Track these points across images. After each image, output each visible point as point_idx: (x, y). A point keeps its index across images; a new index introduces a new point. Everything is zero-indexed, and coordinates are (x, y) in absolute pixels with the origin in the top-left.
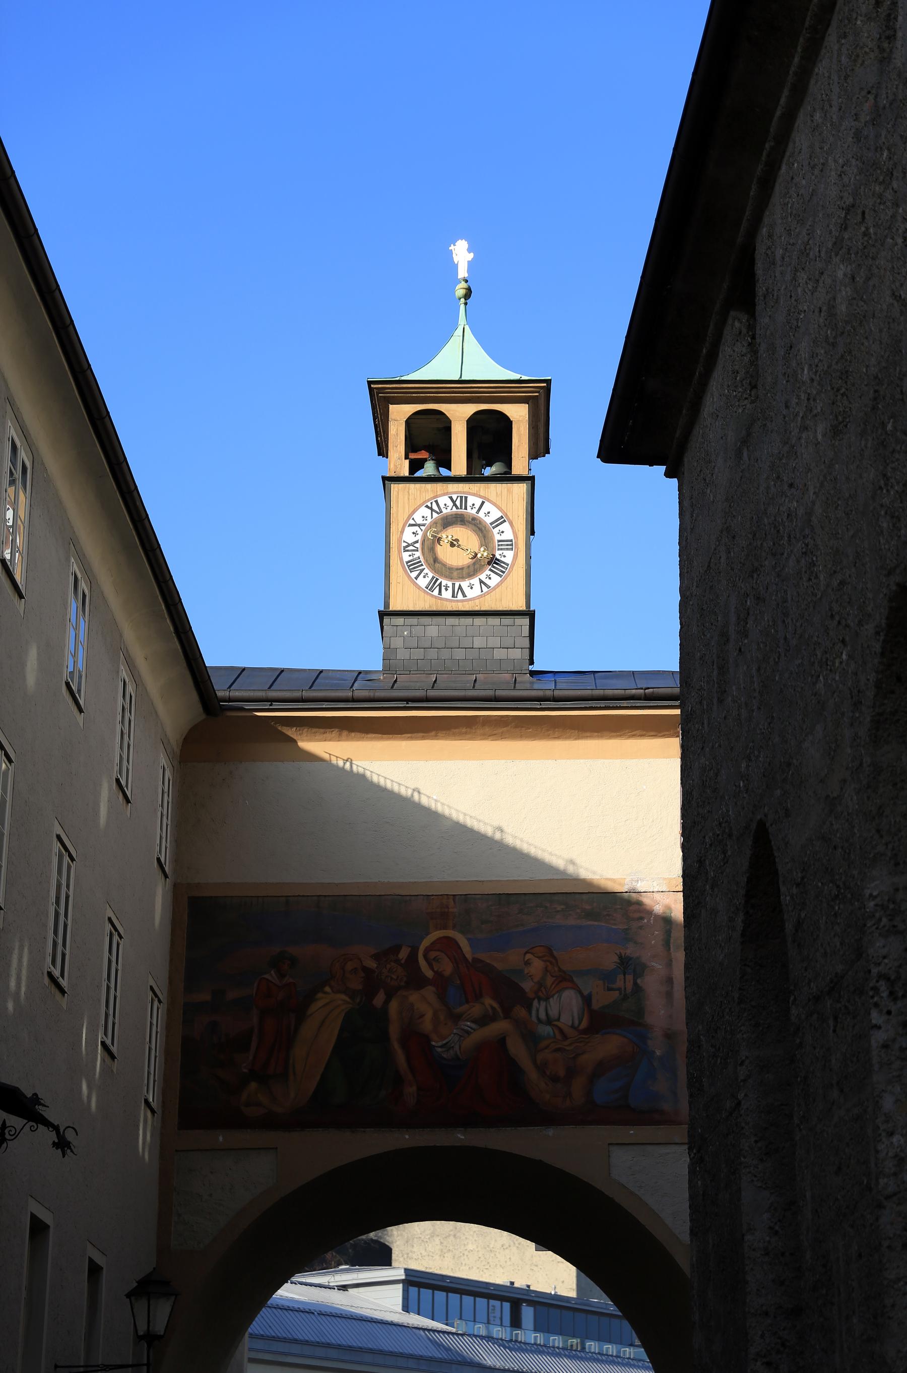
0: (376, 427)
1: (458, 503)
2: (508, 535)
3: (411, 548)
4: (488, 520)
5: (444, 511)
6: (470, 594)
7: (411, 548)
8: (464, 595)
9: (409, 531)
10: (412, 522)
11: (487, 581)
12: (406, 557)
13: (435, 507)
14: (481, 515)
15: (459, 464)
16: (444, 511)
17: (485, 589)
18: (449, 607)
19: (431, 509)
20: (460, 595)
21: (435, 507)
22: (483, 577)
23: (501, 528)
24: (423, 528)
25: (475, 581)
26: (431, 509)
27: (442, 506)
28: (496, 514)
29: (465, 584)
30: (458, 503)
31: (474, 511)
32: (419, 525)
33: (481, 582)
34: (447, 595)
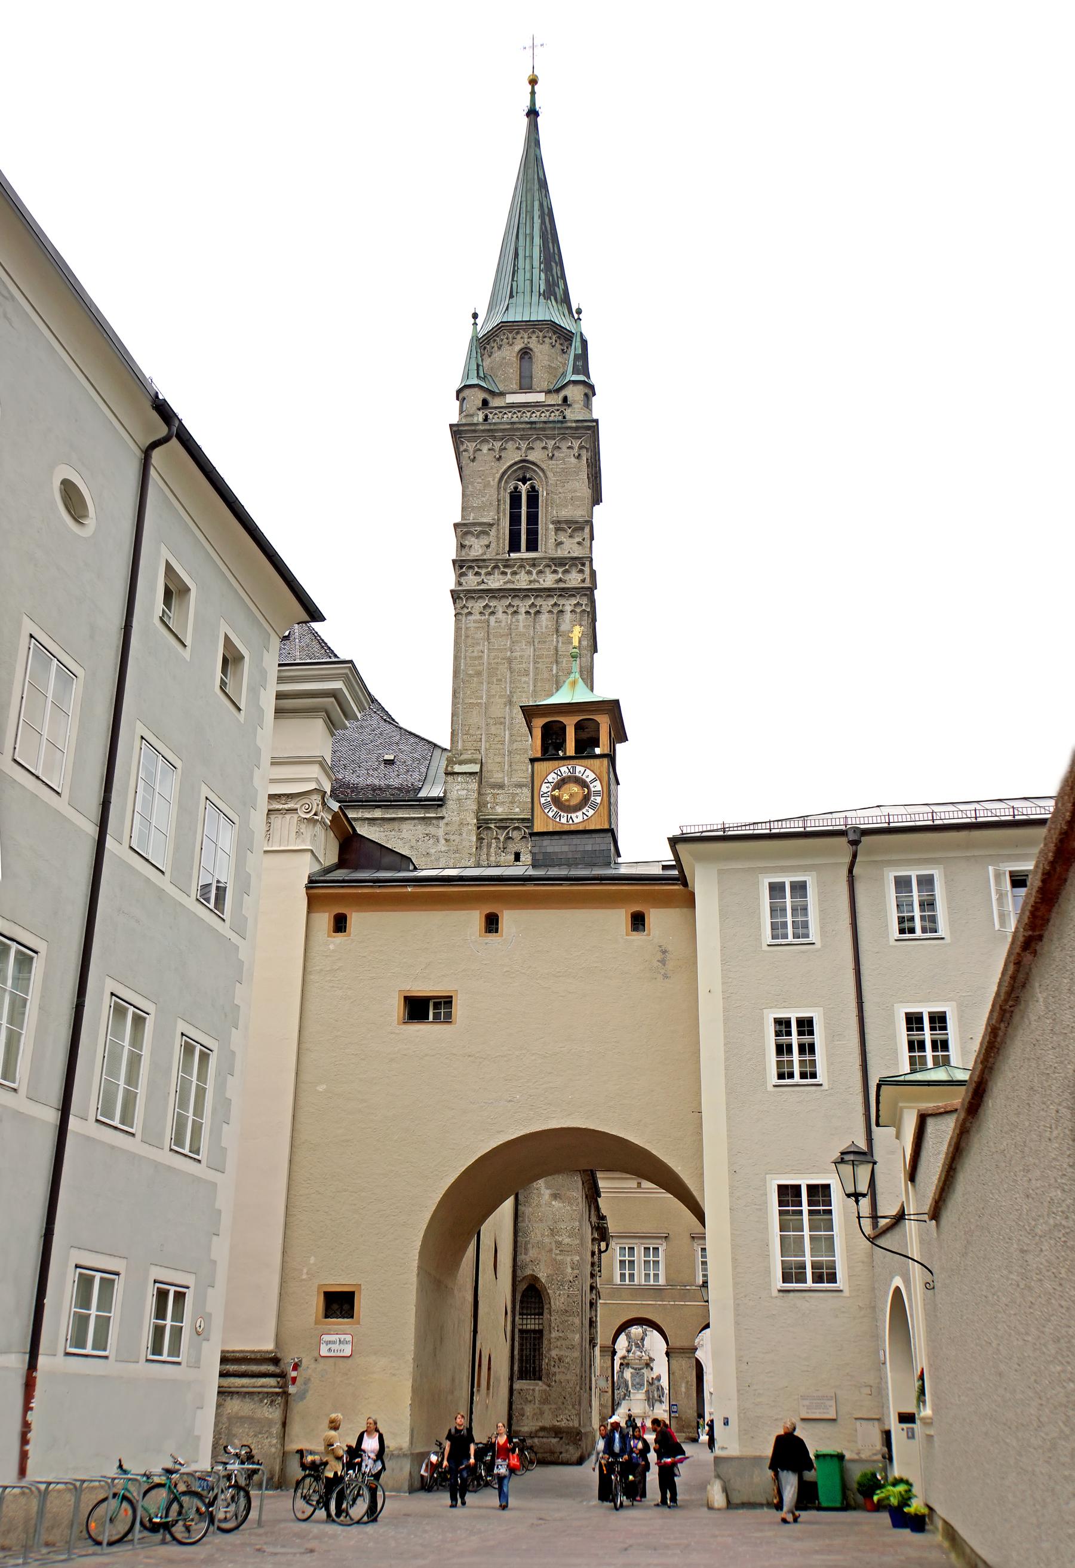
0: (452, 733)
1: (571, 770)
2: (599, 788)
3: (545, 795)
4: (588, 780)
5: (564, 775)
6: (576, 821)
7: (545, 795)
8: (573, 821)
9: (544, 786)
10: (546, 781)
11: (587, 813)
12: (543, 800)
13: (559, 773)
14: (584, 777)
15: (570, 748)
16: (564, 775)
17: (585, 818)
18: (566, 828)
19: (557, 774)
20: (571, 821)
21: (559, 773)
22: (584, 811)
23: (594, 784)
24: (552, 784)
25: (580, 814)
26: (557, 774)
27: (563, 772)
28: (592, 776)
29: (574, 815)
30: (571, 770)
31: (580, 775)
32: (550, 783)
33: (583, 813)
34: (564, 820)
